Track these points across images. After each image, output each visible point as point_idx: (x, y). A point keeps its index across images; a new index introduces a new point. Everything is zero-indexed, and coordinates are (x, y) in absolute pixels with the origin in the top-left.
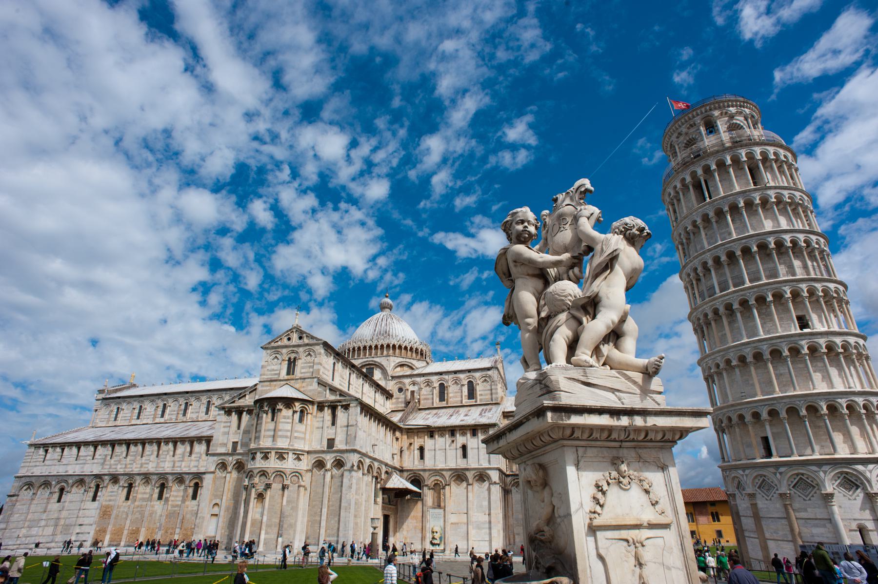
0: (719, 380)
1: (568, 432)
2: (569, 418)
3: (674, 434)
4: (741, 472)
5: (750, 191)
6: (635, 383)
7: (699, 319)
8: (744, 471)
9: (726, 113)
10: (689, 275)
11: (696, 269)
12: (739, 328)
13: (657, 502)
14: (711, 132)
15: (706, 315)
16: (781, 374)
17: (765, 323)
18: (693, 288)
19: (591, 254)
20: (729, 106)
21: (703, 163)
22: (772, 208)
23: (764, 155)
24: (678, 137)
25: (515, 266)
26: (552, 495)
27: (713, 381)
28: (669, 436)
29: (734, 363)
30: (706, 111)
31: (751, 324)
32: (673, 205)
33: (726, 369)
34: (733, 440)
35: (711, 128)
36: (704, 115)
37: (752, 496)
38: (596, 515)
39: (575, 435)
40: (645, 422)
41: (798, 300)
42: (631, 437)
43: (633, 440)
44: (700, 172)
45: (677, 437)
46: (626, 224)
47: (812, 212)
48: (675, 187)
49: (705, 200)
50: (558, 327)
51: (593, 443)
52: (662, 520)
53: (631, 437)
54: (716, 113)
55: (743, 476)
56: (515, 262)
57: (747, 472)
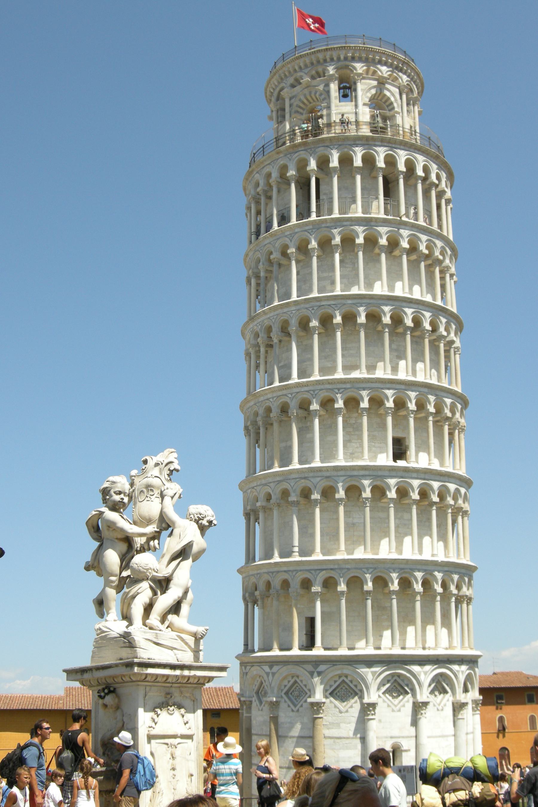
0: (266, 519)
1: (144, 677)
2: (147, 670)
3: (205, 679)
4: (267, 668)
5: (377, 220)
6: (186, 644)
7: (256, 414)
8: (271, 667)
9: (375, 72)
10: (257, 335)
11: (269, 329)
12: (312, 441)
13: (187, 723)
14: (345, 96)
15: (269, 410)
16: (354, 524)
17: (350, 441)
18: (258, 357)
19: (170, 529)
20: (380, 62)
21: (321, 151)
22: (401, 257)
23: (410, 166)
24: (293, 86)
25: (108, 530)
26: (123, 716)
27: (257, 520)
28: (201, 681)
29: (293, 498)
30: (346, 59)
31: (330, 438)
32: (258, 203)
33: (279, 505)
34: (264, 619)
35: (347, 90)
36: (340, 64)
37: (274, 706)
38: (152, 729)
39: (147, 679)
40: (190, 673)
41: (403, 413)
42: (179, 681)
43: (180, 683)
44: (313, 164)
45: (206, 681)
46: (200, 514)
47: (452, 276)
48: (269, 175)
49: (309, 216)
50: (138, 594)
51: (156, 684)
52: (189, 732)
53: (179, 681)
54: (360, 67)
55: (268, 674)
56: (109, 527)
57: (275, 668)
